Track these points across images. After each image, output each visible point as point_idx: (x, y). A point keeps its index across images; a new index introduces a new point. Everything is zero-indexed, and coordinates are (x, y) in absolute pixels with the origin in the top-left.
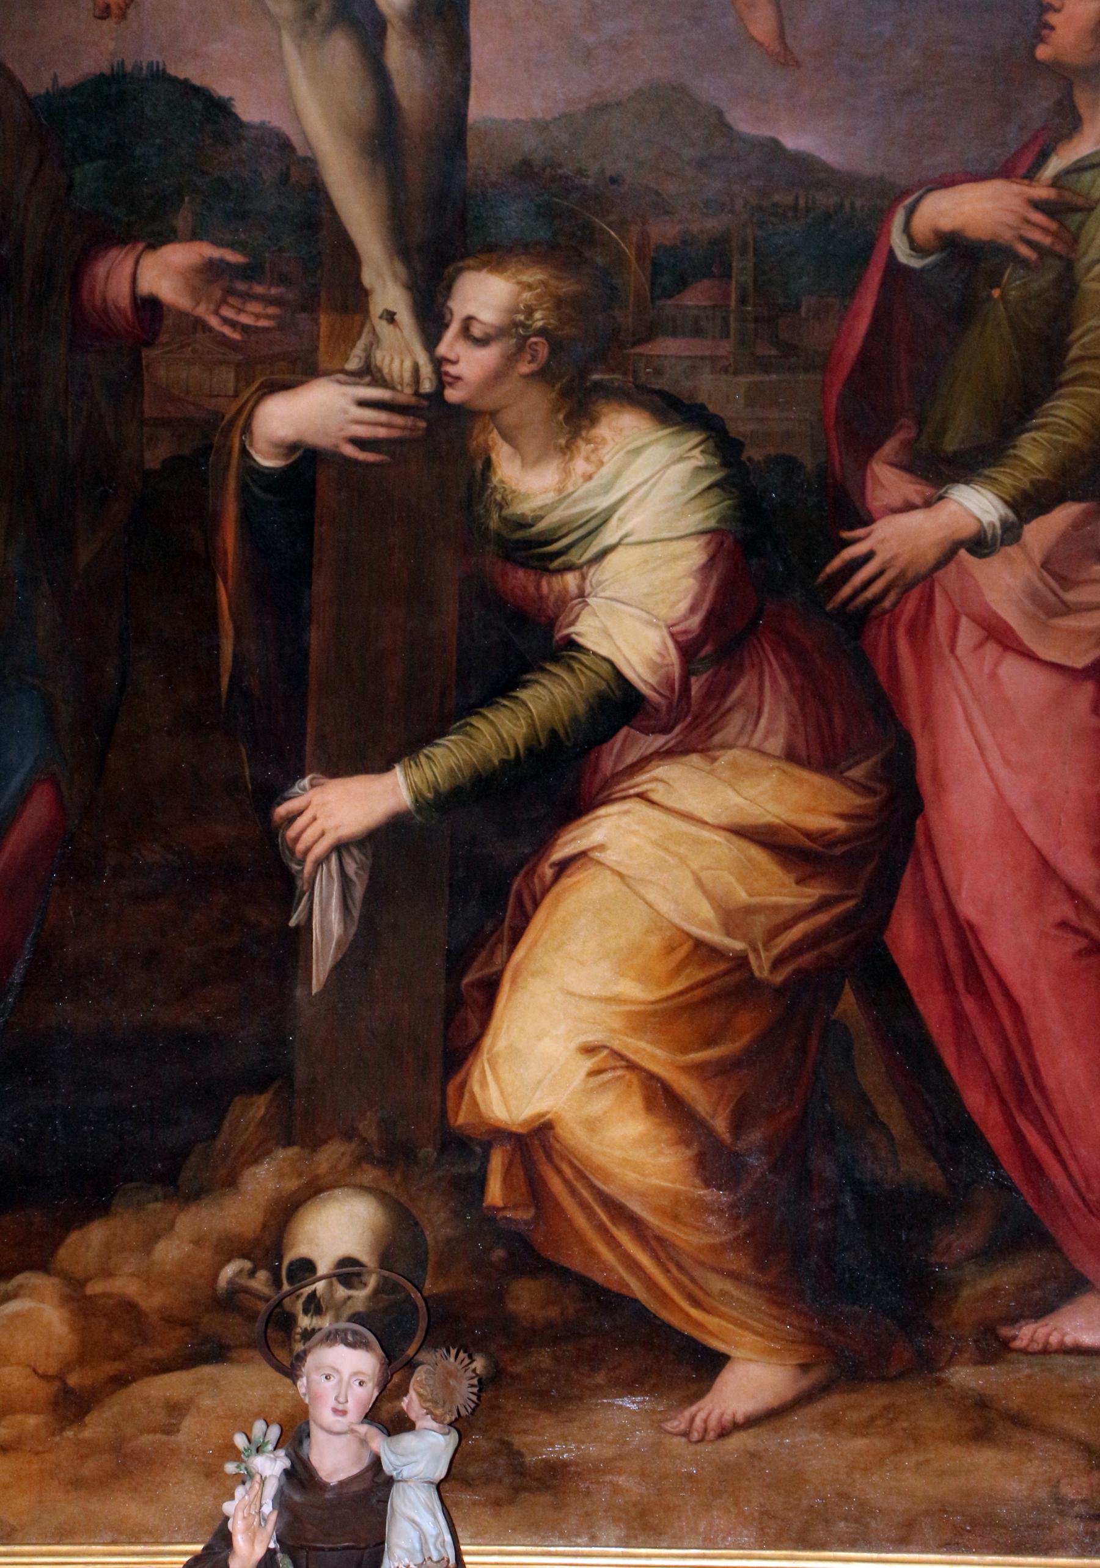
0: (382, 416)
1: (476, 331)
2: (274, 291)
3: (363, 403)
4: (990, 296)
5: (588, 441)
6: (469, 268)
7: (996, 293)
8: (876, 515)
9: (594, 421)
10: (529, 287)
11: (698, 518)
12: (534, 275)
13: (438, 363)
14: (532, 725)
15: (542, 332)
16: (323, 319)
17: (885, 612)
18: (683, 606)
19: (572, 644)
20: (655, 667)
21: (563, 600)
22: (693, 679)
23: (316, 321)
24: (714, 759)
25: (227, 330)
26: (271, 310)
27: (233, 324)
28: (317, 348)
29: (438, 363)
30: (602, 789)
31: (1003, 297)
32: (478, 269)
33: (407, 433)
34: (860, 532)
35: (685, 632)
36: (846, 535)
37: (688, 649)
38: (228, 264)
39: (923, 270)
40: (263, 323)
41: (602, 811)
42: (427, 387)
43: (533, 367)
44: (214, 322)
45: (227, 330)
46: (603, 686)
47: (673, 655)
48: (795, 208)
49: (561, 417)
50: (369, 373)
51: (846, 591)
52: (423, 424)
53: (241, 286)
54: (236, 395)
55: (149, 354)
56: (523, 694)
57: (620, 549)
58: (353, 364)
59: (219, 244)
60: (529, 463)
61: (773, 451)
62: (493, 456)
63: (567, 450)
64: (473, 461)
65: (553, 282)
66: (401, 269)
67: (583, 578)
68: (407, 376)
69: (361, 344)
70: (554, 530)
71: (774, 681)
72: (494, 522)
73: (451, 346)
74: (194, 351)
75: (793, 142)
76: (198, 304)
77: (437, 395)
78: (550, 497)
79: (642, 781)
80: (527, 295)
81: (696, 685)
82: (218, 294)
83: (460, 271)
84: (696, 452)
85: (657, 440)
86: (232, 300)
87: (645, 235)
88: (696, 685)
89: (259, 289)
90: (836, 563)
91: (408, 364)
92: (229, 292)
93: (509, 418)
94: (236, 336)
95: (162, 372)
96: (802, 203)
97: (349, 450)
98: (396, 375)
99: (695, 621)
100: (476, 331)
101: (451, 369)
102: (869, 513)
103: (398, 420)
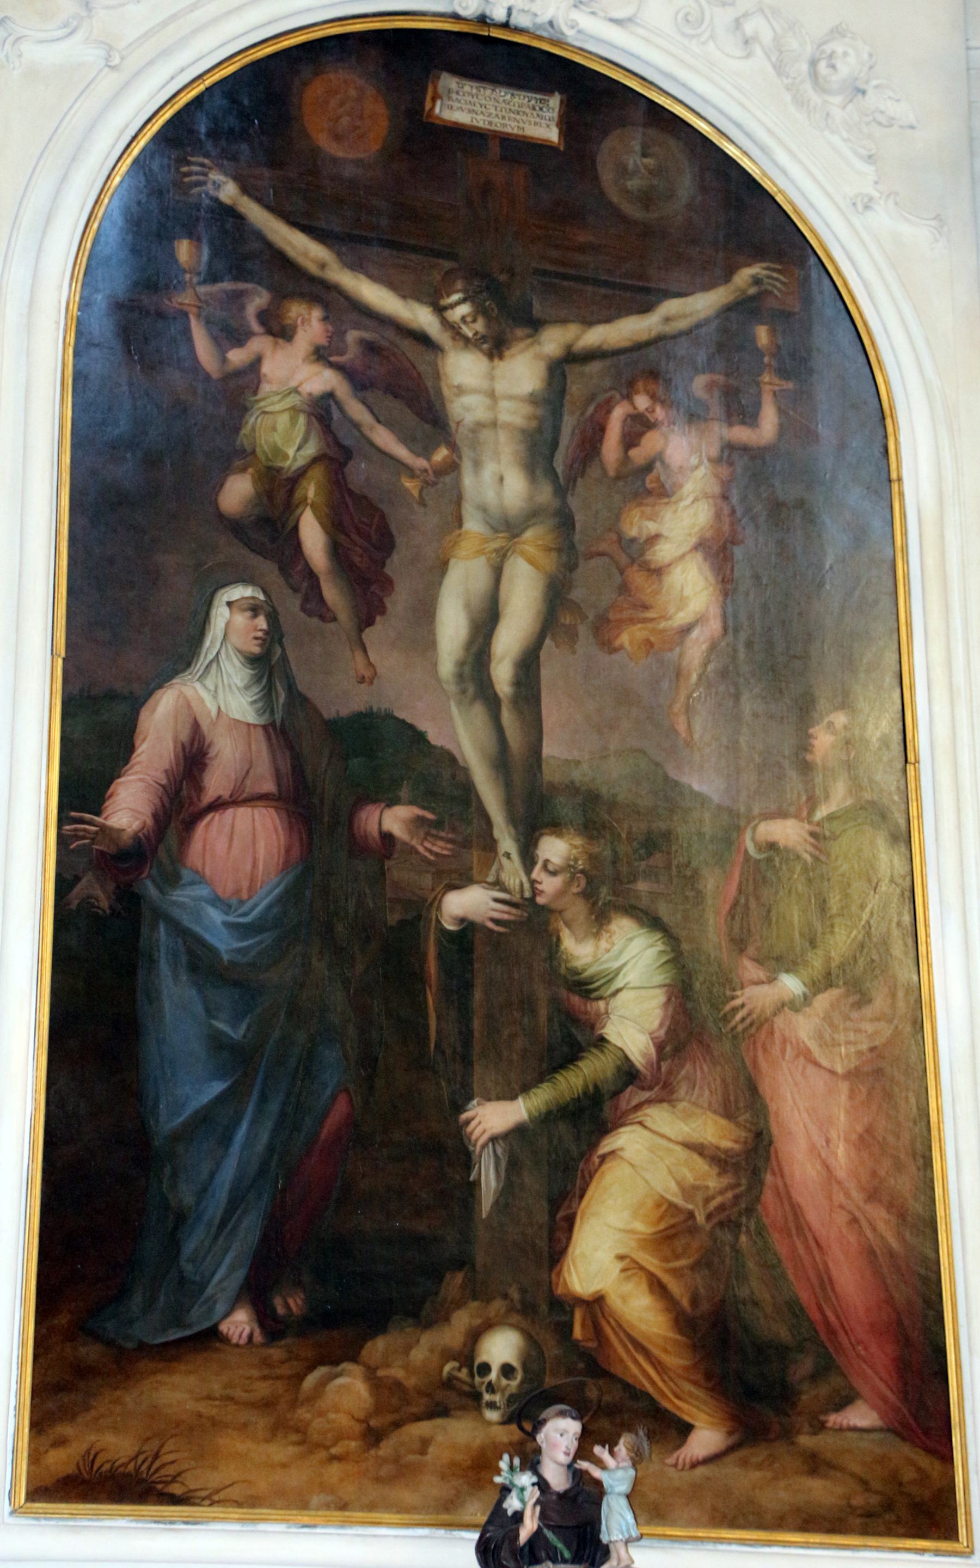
0: (505, 908)
1: (551, 867)
2: (450, 836)
3: (497, 900)
5: (607, 932)
6: (547, 834)
9: (609, 922)
10: (576, 847)
11: (660, 978)
12: (578, 841)
13: (533, 882)
14: (585, 1081)
15: (582, 872)
16: (474, 853)
18: (656, 1024)
19: (602, 1039)
20: (644, 1055)
21: (598, 1015)
22: (662, 1063)
23: (472, 854)
24: (674, 1107)
25: (427, 854)
26: (449, 846)
27: (430, 851)
28: (471, 868)
29: (533, 882)
30: (620, 1117)
32: (551, 834)
33: (518, 919)
35: (657, 1038)
37: (660, 1047)
38: (428, 820)
40: (445, 852)
41: (622, 1130)
42: (527, 894)
43: (579, 889)
44: (421, 849)
45: (427, 854)
46: (619, 1063)
47: (652, 1050)
49: (593, 917)
50: (498, 884)
52: (526, 915)
53: (434, 831)
54: (433, 890)
55: (388, 864)
56: (580, 1064)
57: (624, 991)
58: (491, 879)
59: (424, 808)
60: (579, 940)
62: (561, 934)
63: (597, 935)
64: (551, 935)
65: (586, 846)
66: (512, 831)
67: (607, 1004)
68: (517, 888)
69: (494, 868)
70: (592, 977)
72: (563, 971)
73: (538, 874)
74: (411, 864)
75: (696, 787)
76: (412, 838)
77: (532, 899)
78: (588, 960)
79: (639, 1115)
80: (574, 851)
81: (664, 1067)
82: (422, 834)
83: (542, 835)
84: (659, 943)
85: (639, 935)
86: (429, 838)
87: (630, 827)
88: (664, 1067)
89: (443, 834)
91: (517, 882)
92: (428, 834)
93: (568, 915)
94: (432, 858)
95: (395, 873)
97: (490, 925)
98: (512, 887)
99: (662, 1032)
100: (551, 867)
101: (539, 887)
103: (514, 911)
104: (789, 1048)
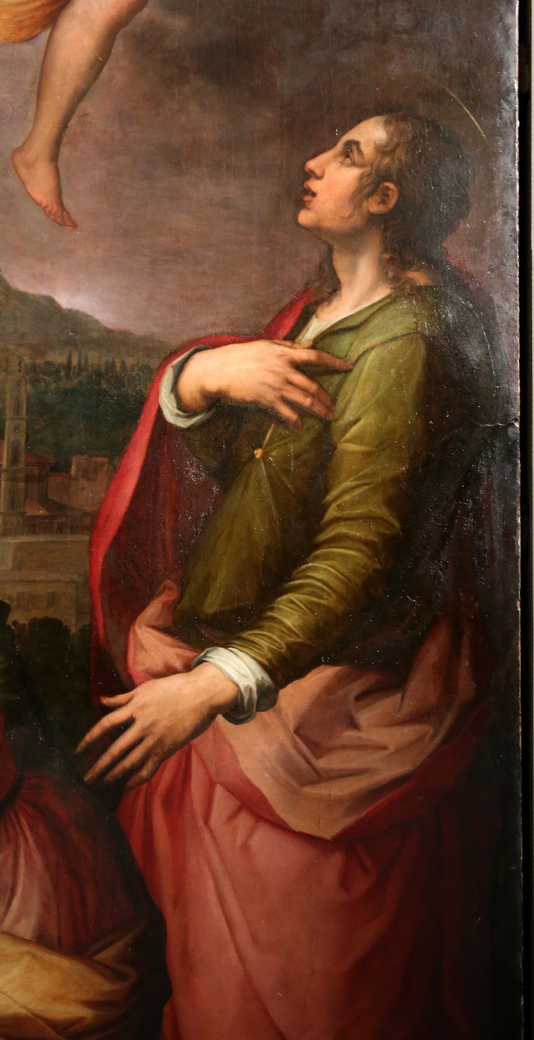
4: (253, 456)
7: (258, 453)
8: (137, 681)
17: (147, 780)
31: (265, 456)
34: (120, 698)
36: (107, 701)
39: (189, 429)
48: (68, 367)
51: (105, 760)
61: (38, 614)
71: (29, 858)
90: (96, 731)
96: (75, 362)
102: (130, 677)
104: (219, 792)
